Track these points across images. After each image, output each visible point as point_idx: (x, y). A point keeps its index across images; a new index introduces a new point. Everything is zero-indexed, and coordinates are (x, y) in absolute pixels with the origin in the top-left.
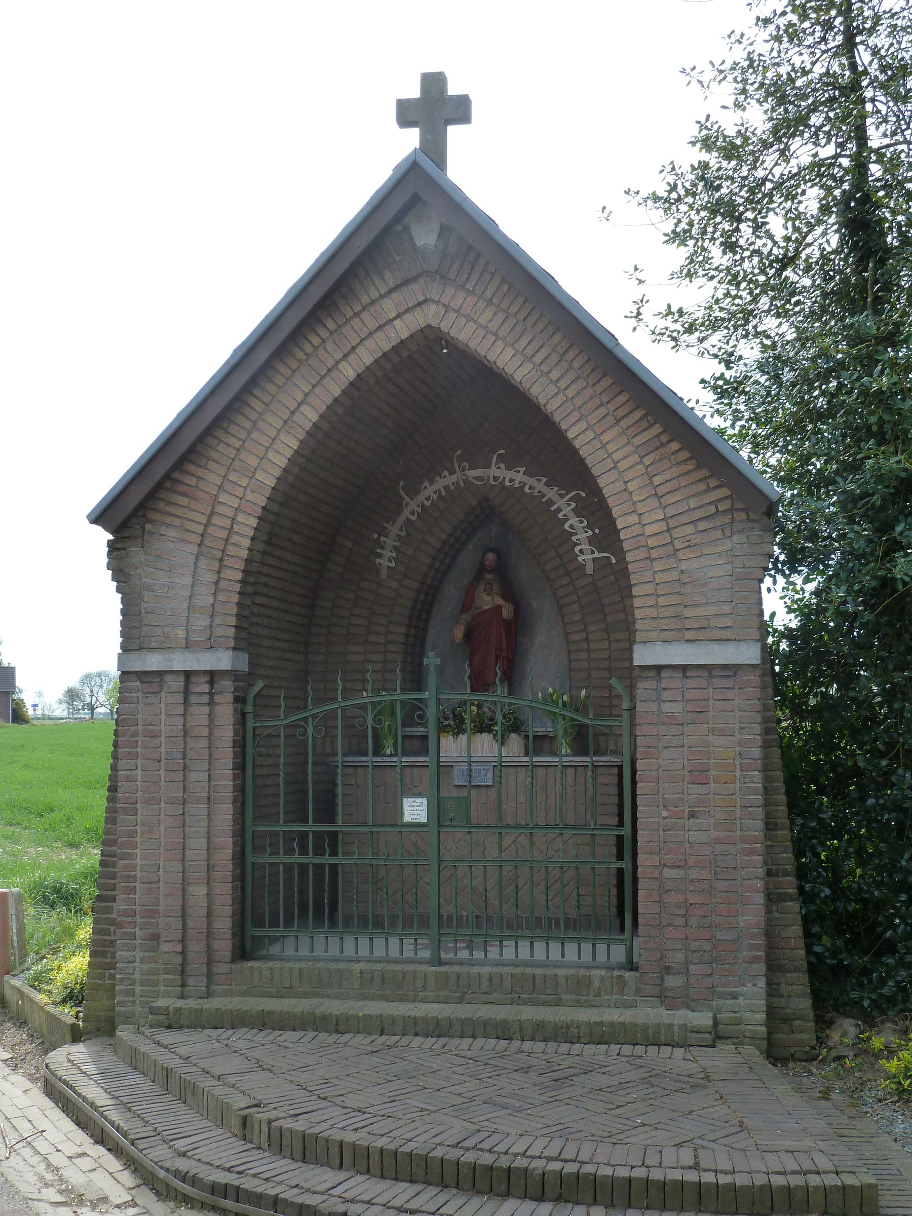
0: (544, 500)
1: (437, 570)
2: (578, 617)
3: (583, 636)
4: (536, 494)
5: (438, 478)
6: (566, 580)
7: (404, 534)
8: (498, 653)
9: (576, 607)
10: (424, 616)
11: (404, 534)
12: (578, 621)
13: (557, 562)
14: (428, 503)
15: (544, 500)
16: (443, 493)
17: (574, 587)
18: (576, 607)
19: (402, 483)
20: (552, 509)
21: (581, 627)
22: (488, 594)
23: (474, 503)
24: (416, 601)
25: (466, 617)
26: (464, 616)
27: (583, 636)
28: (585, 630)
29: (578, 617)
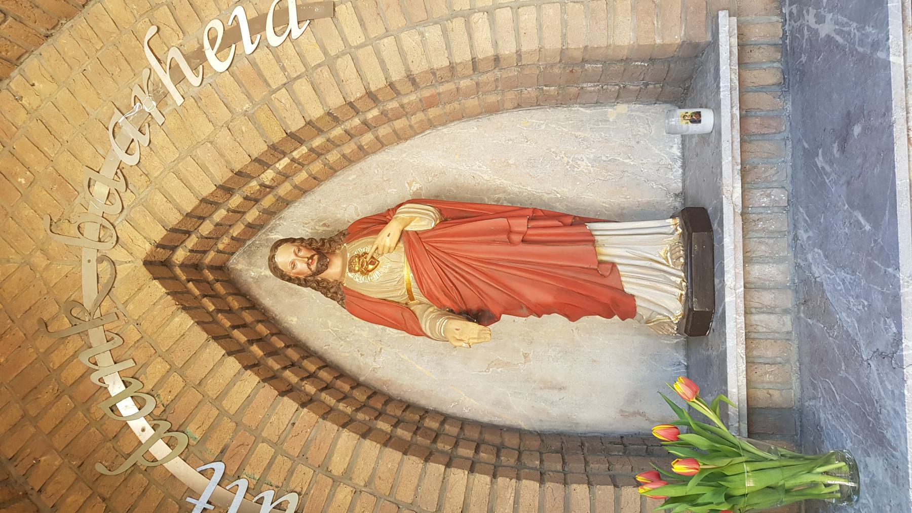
0: (160, 119)
1: (327, 388)
2: (433, 34)
3: (480, 21)
4: (145, 141)
5: (94, 377)
6: (346, 66)
7: (219, 467)
8: (517, 238)
9: (410, 40)
10: (432, 424)
11: (219, 467)
12: (445, 33)
13: (303, 88)
14: (150, 405)
15: (160, 119)
16: (130, 363)
17: (362, 46)
18: (410, 40)
19: (100, 468)
20: (179, 101)
21: (458, 25)
22: (374, 261)
23: (158, 289)
24: (388, 441)
25: (428, 318)
26: (425, 326)
27: (480, 21)
28: (466, 16)
29: (433, 34)
